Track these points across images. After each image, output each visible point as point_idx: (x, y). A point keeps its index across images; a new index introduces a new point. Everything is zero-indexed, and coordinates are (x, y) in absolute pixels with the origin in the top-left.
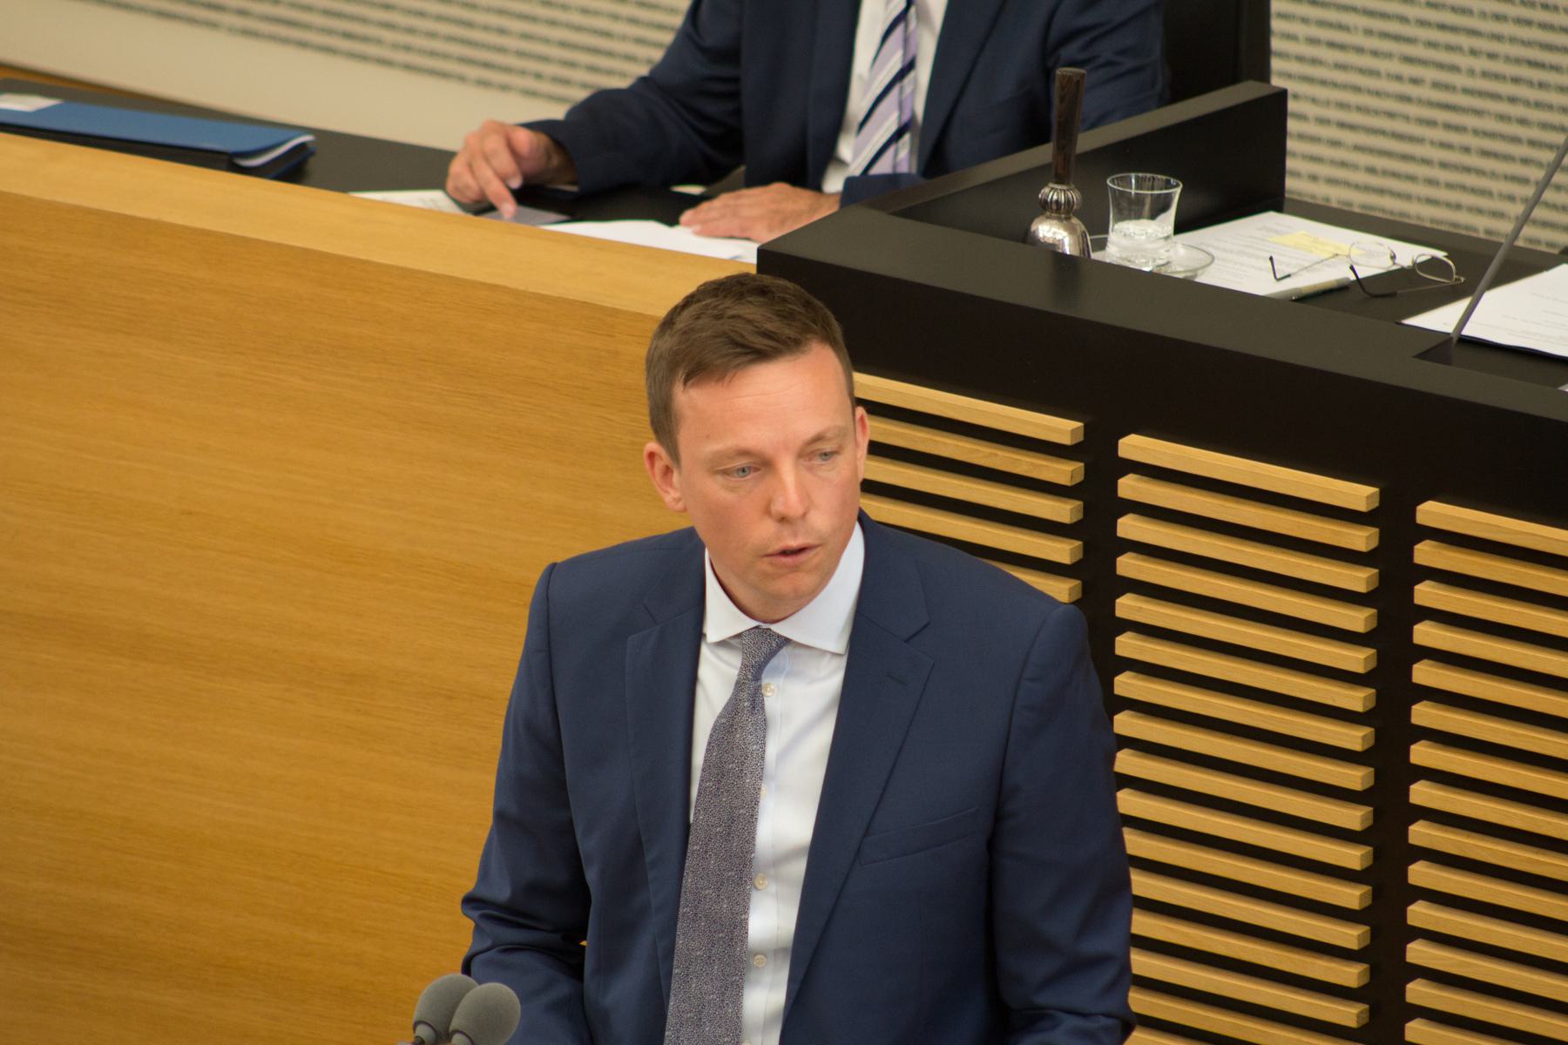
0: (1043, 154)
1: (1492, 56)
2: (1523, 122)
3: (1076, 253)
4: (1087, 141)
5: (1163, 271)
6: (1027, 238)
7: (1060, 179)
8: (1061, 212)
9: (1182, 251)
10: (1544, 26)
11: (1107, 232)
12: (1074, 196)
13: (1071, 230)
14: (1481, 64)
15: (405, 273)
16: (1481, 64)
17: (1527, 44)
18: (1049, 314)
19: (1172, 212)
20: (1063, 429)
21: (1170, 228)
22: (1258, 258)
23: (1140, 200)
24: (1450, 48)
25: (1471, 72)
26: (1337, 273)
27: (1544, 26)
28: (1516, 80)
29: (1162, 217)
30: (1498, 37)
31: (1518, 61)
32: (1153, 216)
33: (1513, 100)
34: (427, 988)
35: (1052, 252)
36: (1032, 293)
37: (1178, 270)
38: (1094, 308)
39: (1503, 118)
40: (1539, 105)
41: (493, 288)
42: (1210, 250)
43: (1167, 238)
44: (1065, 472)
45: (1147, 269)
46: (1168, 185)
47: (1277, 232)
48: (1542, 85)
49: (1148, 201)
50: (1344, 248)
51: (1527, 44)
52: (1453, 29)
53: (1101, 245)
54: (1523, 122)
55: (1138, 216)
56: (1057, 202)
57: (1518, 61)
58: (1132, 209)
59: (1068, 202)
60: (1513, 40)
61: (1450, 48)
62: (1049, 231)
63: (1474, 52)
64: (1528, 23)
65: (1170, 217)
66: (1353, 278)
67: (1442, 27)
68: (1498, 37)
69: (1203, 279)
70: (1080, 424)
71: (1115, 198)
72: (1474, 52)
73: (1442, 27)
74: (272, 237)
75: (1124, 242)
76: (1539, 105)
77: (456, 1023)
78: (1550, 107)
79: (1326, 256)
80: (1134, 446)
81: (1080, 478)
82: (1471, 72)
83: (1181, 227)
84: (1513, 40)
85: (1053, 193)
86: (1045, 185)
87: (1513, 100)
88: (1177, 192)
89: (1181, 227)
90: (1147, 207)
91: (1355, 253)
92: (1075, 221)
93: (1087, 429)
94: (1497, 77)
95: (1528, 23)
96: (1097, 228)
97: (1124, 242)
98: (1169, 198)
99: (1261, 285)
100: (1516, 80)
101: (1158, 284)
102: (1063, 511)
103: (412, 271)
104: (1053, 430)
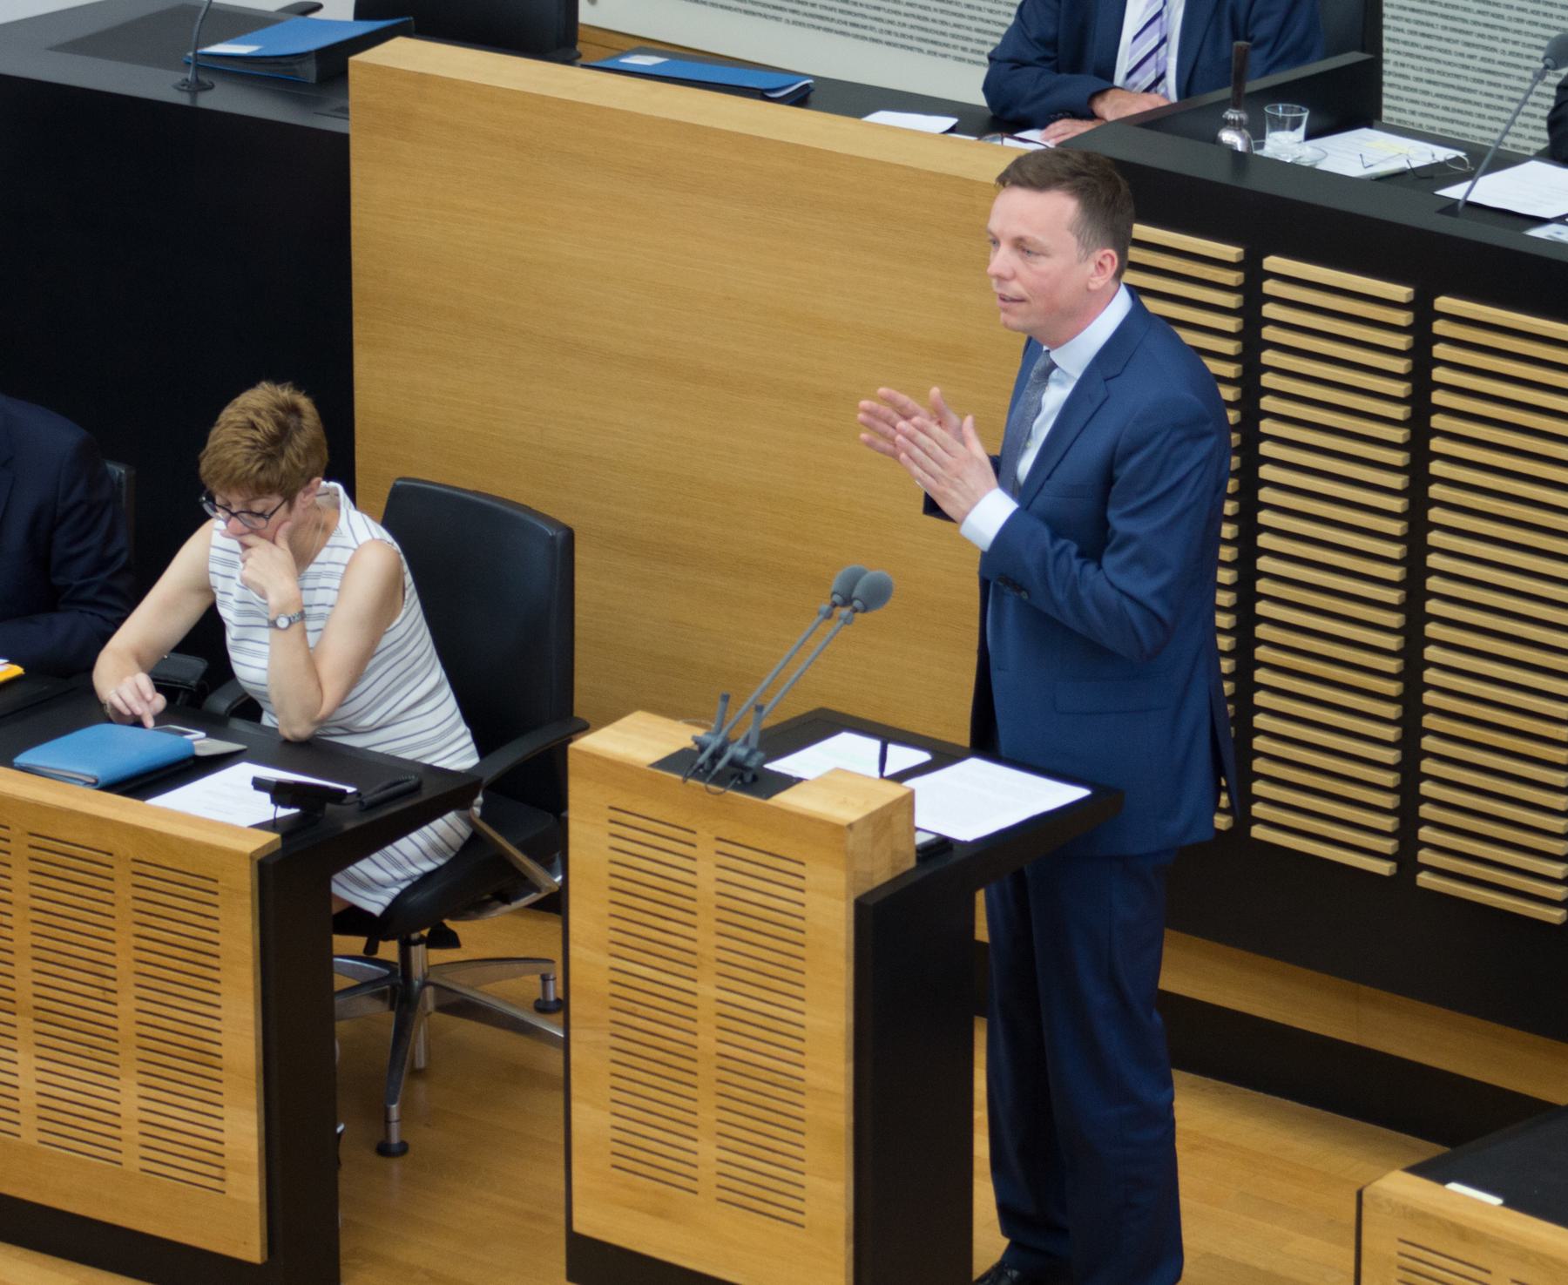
0: (1226, 93)
4: (1252, 86)
6: (1216, 141)
7: (1236, 106)
8: (1236, 126)
11: (1263, 137)
12: (1244, 116)
13: (1242, 137)
15: (852, 158)
18: (1227, 186)
23: (1284, 120)
34: (840, 573)
35: (1230, 149)
36: (1220, 173)
38: (1256, 182)
53: (1261, 146)
55: (1283, 129)
58: (1279, 125)
59: (1241, 121)
62: (1228, 136)
65: (1302, 130)
70: (1240, 250)
77: (856, 593)
80: (1272, 263)
81: (1241, 281)
83: (1309, 136)
85: (1231, 115)
88: (1306, 115)
89: (1309, 136)
93: (1247, 253)
96: (1258, 135)
99: (1354, 169)
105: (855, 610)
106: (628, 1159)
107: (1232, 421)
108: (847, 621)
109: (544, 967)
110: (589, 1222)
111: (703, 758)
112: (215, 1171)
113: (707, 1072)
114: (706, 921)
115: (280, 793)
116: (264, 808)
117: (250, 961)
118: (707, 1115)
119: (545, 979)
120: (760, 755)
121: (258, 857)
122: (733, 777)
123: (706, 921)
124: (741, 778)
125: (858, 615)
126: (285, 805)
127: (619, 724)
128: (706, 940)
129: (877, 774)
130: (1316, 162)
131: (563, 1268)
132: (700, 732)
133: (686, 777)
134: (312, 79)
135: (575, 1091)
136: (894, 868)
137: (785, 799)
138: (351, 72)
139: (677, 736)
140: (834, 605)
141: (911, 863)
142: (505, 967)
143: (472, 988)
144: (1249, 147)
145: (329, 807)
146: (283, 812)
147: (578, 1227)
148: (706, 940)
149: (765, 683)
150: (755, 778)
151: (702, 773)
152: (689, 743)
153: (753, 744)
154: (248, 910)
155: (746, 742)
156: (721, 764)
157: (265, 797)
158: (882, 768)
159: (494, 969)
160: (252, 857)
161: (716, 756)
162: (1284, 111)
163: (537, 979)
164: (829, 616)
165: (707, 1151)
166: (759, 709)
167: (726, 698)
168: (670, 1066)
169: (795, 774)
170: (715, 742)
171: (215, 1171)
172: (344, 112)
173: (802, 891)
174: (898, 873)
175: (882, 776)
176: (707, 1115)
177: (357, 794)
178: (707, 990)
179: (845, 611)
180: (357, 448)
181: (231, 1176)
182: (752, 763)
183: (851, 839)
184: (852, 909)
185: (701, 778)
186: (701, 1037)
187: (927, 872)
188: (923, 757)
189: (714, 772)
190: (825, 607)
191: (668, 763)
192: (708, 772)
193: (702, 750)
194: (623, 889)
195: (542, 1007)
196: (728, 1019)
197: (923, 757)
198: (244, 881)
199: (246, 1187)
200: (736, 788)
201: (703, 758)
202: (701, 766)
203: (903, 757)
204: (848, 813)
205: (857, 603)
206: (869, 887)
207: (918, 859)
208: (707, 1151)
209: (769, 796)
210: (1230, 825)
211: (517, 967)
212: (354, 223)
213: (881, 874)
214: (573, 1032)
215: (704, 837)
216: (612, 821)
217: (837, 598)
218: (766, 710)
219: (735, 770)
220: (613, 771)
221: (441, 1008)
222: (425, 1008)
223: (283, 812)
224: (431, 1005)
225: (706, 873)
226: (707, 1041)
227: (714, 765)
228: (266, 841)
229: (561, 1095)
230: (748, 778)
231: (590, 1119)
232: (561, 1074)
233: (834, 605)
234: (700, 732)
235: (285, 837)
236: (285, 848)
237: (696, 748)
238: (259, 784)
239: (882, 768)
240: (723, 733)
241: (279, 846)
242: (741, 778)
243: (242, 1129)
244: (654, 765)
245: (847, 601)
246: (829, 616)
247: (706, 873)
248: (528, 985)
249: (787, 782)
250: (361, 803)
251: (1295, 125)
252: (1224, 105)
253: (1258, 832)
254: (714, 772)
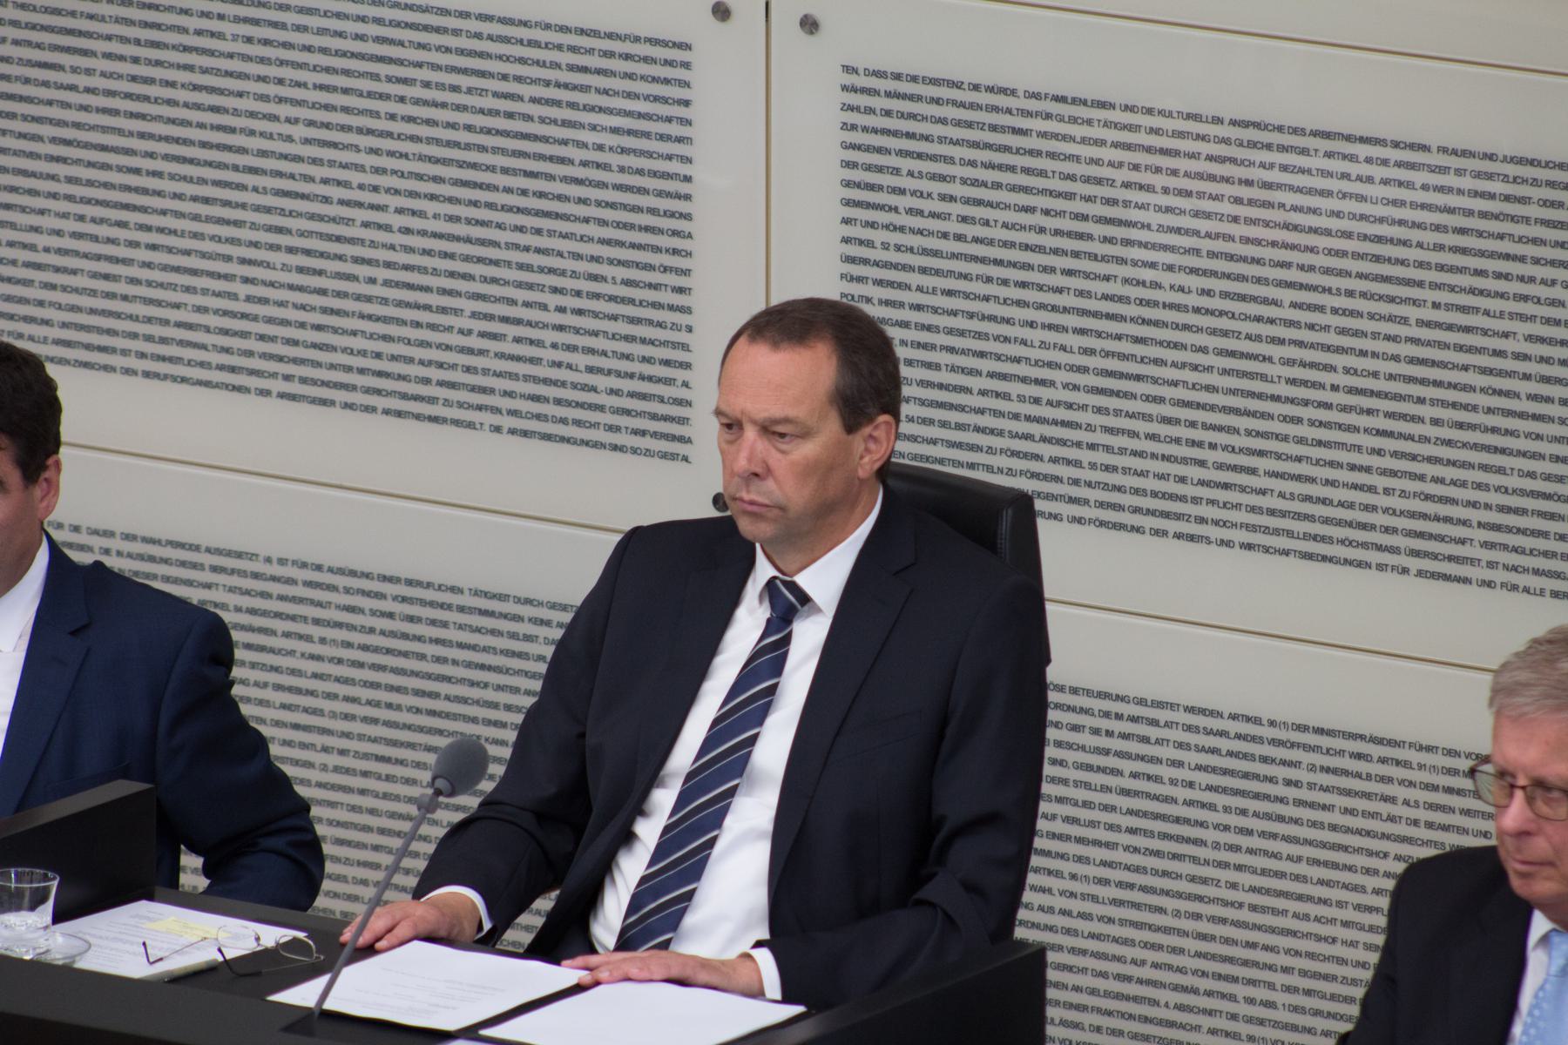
1: (342, 752)
2: (372, 812)
5: (43, 958)
9: (60, 939)
10: (388, 724)
14: (333, 760)
16: (333, 760)
17: (375, 740)
19: (50, 903)
21: (48, 919)
22: (132, 943)
23: (19, 893)
24: (304, 746)
25: (324, 768)
26: (205, 955)
27: (388, 724)
28: (365, 774)
29: (41, 908)
30: (347, 735)
31: (366, 756)
32: (32, 908)
33: (363, 792)
37: (57, 957)
39: (354, 809)
40: (386, 796)
42: (88, 938)
43: (46, 928)
45: (27, 957)
46: (45, 878)
47: (149, 919)
48: (389, 778)
49: (27, 894)
50: (212, 933)
51: (375, 740)
52: (306, 728)
54: (372, 812)
55: (18, 908)
57: (366, 756)
60: (361, 737)
61: (304, 746)
63: (325, 749)
64: (375, 721)
65: (49, 906)
66: (221, 959)
67: (296, 727)
68: (347, 735)
69: (82, 964)
72: (325, 749)
73: (296, 727)
76: (386, 796)
78: (397, 798)
79: (195, 939)
82: (324, 768)
83: (58, 918)
84: (361, 737)
87: (363, 792)
88: (55, 884)
89: (58, 918)
90: (27, 899)
91: (222, 936)
94: (348, 771)
95: (375, 721)
98: (46, 891)
99: (135, 968)
100: (365, 774)
130: (74, 957)
162: (19, 879)
251: (37, 901)
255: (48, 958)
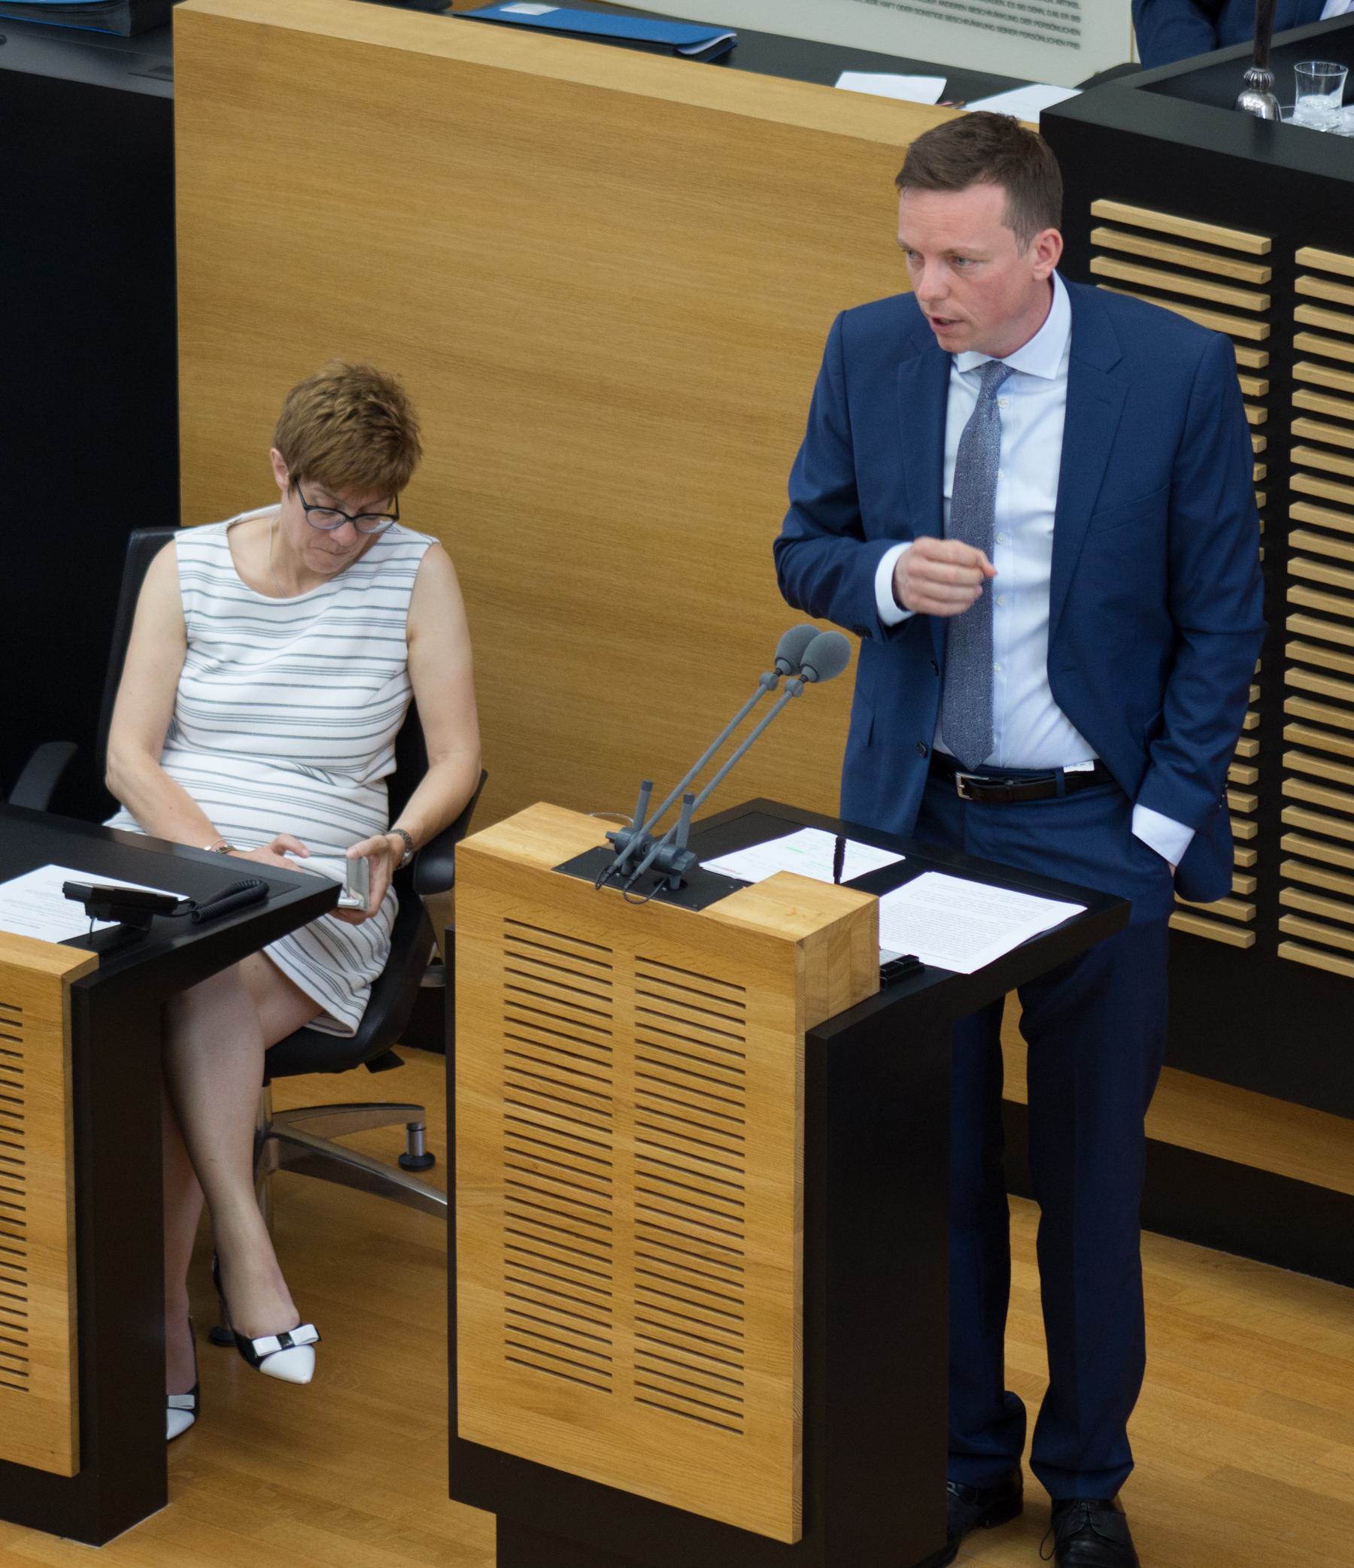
0: (1247, 47)
3: (1271, 117)
4: (1278, 39)
5: (1335, 131)
6: (1235, 106)
7: (1259, 65)
8: (1260, 88)
9: (1348, 118)
11: (1293, 102)
12: (1269, 76)
13: (1267, 101)
15: (791, 128)
20: (1256, 243)
23: (1318, 80)
29: (1333, 94)
34: (785, 635)
36: (1239, 146)
38: (1283, 157)
41: (852, 139)
44: (1257, 274)
46: (1338, 70)
49: (1323, 82)
53: (1290, 113)
55: (1316, 92)
56: (1257, 81)
58: (1312, 87)
59: (1265, 81)
62: (1250, 101)
65: (1338, 95)
70: (1267, 240)
71: (1300, 80)
74: (697, 103)
75: (1307, 111)
77: (805, 659)
80: (1307, 255)
81: (1268, 278)
85: (1254, 74)
86: (1248, 68)
88: (1344, 75)
90: (1323, 86)
92: (1269, 95)
93: (1274, 244)
96: (1285, 99)
97: (1307, 111)
98: (1337, 80)
101: (1331, 140)
102: (1256, 302)
103: (796, 127)
104: (1252, 244)
105: (805, 680)
106: (524, 1348)
107: (1256, 449)
108: (795, 693)
109: (411, 1115)
110: (478, 1425)
111: (619, 860)
112: (16, 1364)
113: (623, 1241)
114: (623, 1057)
115: (96, 902)
116: (78, 920)
117: (62, 1107)
118: (624, 1296)
119: (412, 1129)
120: (691, 856)
121: (72, 981)
122: (656, 884)
123: (623, 1057)
124: (667, 884)
125: (808, 686)
126: (101, 919)
127: (514, 818)
128: (623, 1083)
129: (832, 880)
131: (445, 1484)
132: (616, 828)
133: (599, 884)
134: (126, 31)
135: (461, 1265)
136: (854, 994)
137: (724, 909)
138: (177, 23)
139: (589, 833)
140: (780, 673)
141: (875, 988)
142: (364, 1113)
143: (325, 1140)
144: (1275, 112)
145: (157, 919)
146: (100, 925)
147: (463, 1433)
148: (623, 1083)
149: (695, 768)
150: (683, 884)
151: (622, 878)
152: (602, 841)
153: (682, 841)
154: (60, 1044)
155: (672, 841)
156: (642, 867)
157: (80, 907)
158: (837, 872)
159: (352, 1115)
160: (63, 980)
161: (636, 856)
162: (1317, 70)
163: (402, 1130)
164: (772, 686)
165: (624, 1340)
166: (689, 799)
167: (648, 787)
168: (577, 1235)
169: (735, 876)
170: (635, 841)
171: (16, 1364)
172: (166, 72)
173: (742, 1022)
174: (859, 1000)
175: (837, 881)
176: (624, 1296)
177: (190, 903)
178: (624, 1142)
179: (792, 681)
180: (182, 482)
181: (37, 1371)
182: (681, 866)
183: (802, 958)
184: (803, 1043)
185: (620, 886)
186: (616, 1201)
187: (890, 1000)
188: (891, 858)
189: (633, 878)
190: (768, 675)
191: (574, 866)
192: (627, 876)
193: (619, 850)
194: (521, 1018)
195: (415, 1163)
196: (650, 1178)
197: (891, 858)
198: (55, 1009)
199: (55, 1383)
200: (660, 896)
201: (619, 860)
202: (618, 869)
203: (865, 858)
204: (798, 929)
205: (806, 671)
206: (823, 1018)
207: (882, 982)
208: (624, 1340)
209: (699, 909)
210: (1252, 942)
211: (379, 1114)
212: (180, 207)
213: (838, 1001)
214: (459, 1194)
215: (621, 955)
216: (508, 937)
217: (782, 664)
218: (696, 801)
219: (658, 874)
220: (512, 875)
221: (288, 1165)
222: (267, 1164)
223: (100, 925)
224: (274, 1162)
225: (624, 1000)
226: (624, 1206)
227: (634, 869)
228: (81, 961)
229: (443, 1276)
230: (675, 884)
231: (480, 1299)
232: (444, 1247)
233: (780, 673)
234: (616, 828)
235: (103, 955)
236: (101, 970)
237: (612, 847)
238: (71, 892)
239: (837, 872)
240: (646, 827)
241: (96, 967)
242: (667, 884)
243: (49, 1312)
244: (558, 868)
245: (795, 668)
246: (772, 686)
247: (624, 1000)
248: (390, 1138)
249: (728, 886)
250: (195, 914)
251: (1331, 88)
252: (1244, 63)
253: (1287, 951)
254: (633, 878)
255: (1338, 131)
